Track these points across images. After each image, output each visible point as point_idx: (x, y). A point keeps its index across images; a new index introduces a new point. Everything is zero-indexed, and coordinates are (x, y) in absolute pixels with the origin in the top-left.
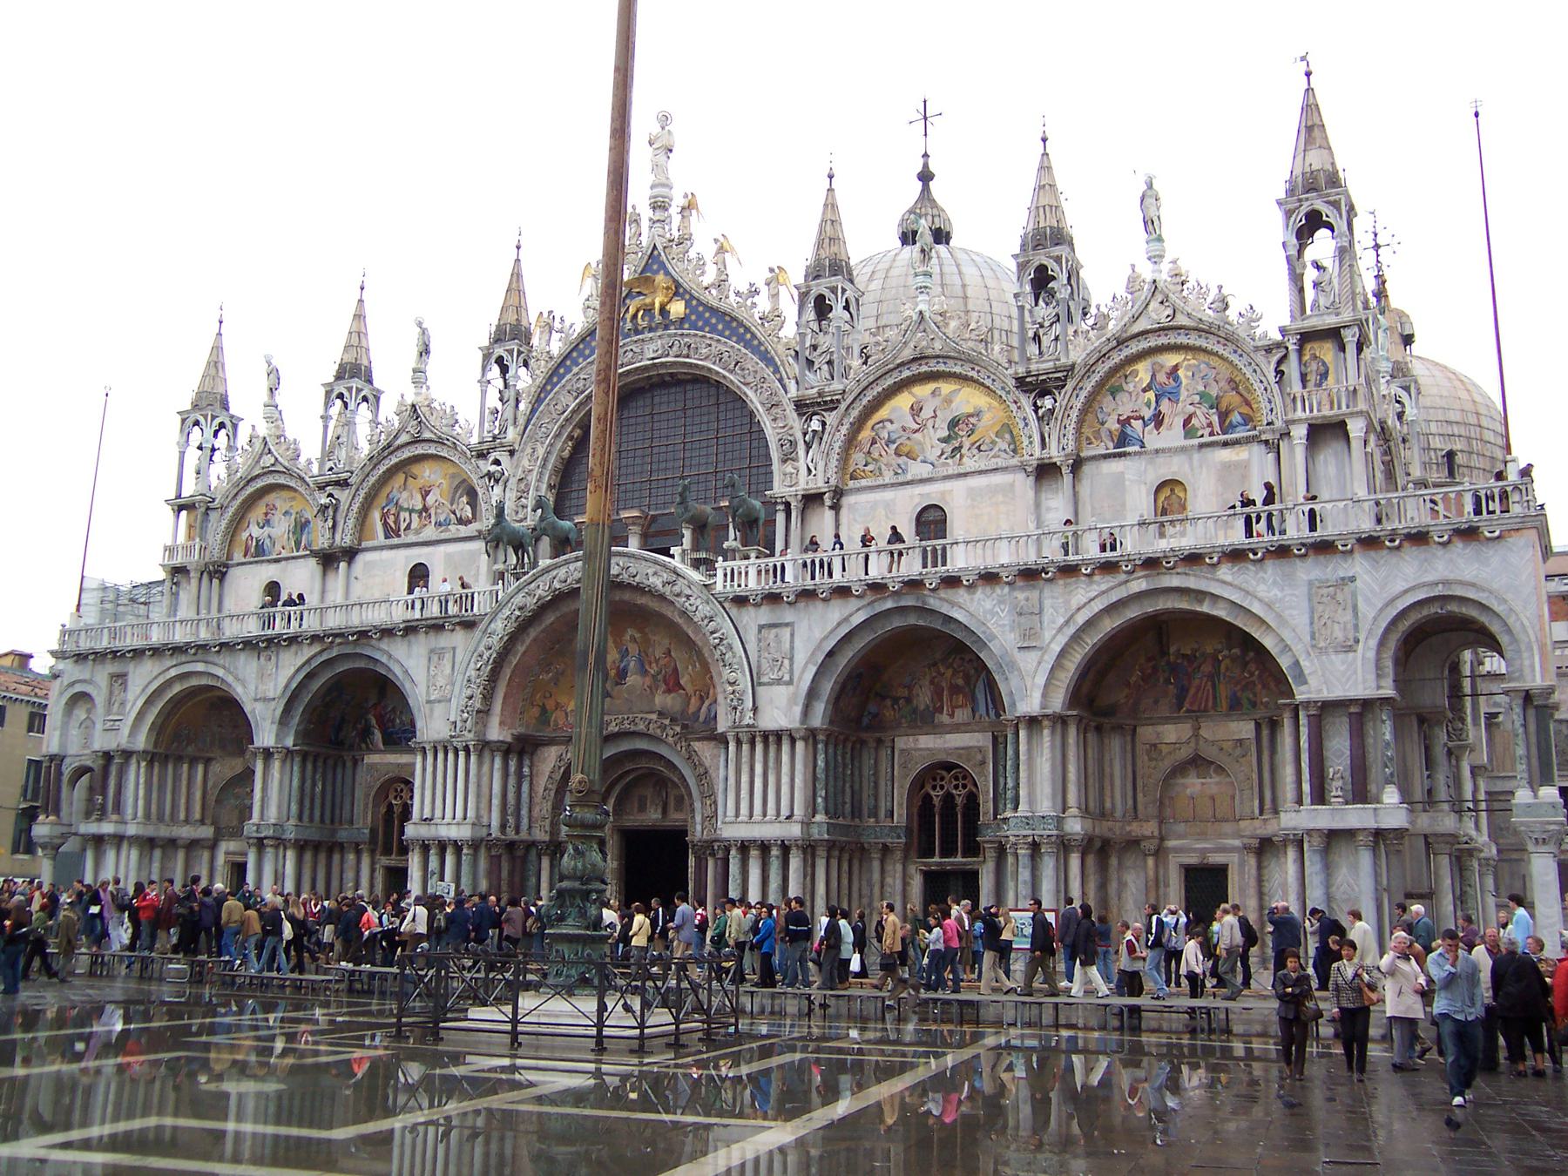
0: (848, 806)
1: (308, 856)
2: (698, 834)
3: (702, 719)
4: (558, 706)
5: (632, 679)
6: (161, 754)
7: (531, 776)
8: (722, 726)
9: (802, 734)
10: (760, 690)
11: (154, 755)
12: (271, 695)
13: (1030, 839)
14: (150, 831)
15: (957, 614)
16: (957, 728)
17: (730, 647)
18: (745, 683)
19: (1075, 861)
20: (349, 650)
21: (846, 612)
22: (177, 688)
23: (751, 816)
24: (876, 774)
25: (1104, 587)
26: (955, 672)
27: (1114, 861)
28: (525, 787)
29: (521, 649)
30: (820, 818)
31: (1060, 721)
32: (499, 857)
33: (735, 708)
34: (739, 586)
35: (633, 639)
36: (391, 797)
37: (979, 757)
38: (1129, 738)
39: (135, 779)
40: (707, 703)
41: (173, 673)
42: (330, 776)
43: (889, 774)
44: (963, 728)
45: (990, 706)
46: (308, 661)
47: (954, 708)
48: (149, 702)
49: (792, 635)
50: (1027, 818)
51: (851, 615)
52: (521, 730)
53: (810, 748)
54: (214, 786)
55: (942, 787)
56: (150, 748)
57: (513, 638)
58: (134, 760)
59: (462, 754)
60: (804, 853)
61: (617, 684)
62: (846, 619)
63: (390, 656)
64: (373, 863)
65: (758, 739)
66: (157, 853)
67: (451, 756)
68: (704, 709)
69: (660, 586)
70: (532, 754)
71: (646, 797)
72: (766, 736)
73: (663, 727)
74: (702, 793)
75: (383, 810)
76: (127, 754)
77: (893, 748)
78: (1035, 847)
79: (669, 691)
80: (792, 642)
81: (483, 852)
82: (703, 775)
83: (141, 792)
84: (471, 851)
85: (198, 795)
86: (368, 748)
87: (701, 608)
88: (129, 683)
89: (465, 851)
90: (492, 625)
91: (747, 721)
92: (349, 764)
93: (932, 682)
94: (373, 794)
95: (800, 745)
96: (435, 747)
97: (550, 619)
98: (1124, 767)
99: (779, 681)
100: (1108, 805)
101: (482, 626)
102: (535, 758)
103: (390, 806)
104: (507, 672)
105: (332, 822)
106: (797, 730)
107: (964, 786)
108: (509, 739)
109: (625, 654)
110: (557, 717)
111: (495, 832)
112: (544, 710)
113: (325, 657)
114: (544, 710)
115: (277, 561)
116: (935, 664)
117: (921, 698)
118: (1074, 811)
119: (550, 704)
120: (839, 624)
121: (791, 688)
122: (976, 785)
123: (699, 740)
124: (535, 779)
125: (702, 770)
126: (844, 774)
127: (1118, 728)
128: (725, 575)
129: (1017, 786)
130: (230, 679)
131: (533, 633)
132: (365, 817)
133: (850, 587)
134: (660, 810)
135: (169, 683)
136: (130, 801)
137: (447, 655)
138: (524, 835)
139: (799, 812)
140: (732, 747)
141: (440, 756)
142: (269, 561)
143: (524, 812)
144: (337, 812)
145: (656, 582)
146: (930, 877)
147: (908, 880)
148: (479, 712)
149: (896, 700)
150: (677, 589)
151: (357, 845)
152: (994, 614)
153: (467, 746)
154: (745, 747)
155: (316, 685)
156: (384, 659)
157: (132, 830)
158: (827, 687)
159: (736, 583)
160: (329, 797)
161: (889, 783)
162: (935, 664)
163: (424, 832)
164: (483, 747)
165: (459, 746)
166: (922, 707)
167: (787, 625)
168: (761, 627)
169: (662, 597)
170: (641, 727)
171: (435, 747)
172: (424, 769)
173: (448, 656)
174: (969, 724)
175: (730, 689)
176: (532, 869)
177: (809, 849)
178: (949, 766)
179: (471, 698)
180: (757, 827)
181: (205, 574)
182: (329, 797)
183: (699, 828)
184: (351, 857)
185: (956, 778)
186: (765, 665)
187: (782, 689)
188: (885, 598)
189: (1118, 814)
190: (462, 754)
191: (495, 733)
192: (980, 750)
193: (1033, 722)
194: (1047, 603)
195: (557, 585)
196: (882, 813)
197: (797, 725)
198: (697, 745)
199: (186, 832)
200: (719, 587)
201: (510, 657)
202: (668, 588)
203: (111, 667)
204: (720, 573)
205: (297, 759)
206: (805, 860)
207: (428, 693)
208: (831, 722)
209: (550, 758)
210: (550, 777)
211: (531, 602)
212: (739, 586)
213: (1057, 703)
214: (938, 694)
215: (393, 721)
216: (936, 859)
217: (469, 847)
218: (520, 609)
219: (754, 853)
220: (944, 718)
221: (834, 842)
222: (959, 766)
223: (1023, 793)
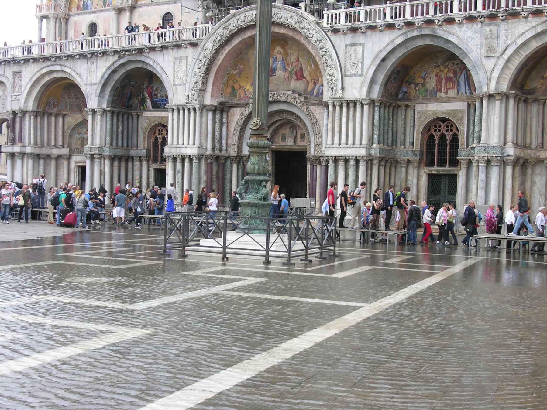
0: (390, 140)
1: (116, 163)
2: (312, 153)
3: (315, 94)
4: (240, 87)
7: (227, 123)
8: (326, 97)
9: (367, 102)
10: (346, 79)
13: (486, 158)
14: (37, 151)
15: (451, 38)
16: (448, 100)
17: (330, 56)
18: (338, 75)
19: (509, 170)
20: (132, 58)
21: (392, 37)
22: (47, 79)
23: (340, 144)
24: (405, 123)
25: (534, 24)
26: (449, 70)
27: (529, 171)
28: (224, 129)
29: (221, 57)
30: (375, 145)
31: (506, 96)
32: (212, 164)
33: (333, 88)
34: (336, 23)
35: (279, 52)
36: (157, 134)
37: (460, 115)
38: (541, 106)
39: (29, 124)
40: (317, 86)
41: (45, 71)
42: (125, 123)
43: (412, 123)
44: (452, 100)
45: (467, 88)
46: (113, 64)
47: (447, 89)
48: (33, 86)
49: (363, 50)
50: (485, 147)
51: (394, 39)
52: (223, 100)
53: (371, 109)
54: (68, 129)
55: (440, 131)
56: (35, 109)
57: (217, 52)
58: (27, 115)
59: (192, 112)
60: (367, 163)
62: (393, 41)
63: (154, 61)
64: (148, 167)
65: (344, 105)
66: (42, 161)
68: (316, 89)
69: (293, 24)
70: (228, 112)
71: (285, 134)
72: (348, 104)
73: (295, 99)
74: (314, 132)
75: (153, 140)
76: (24, 112)
77: (415, 110)
78: (488, 162)
79: (298, 79)
80: (363, 53)
81: (203, 162)
82: (315, 124)
83: (32, 131)
84: (197, 161)
85: (60, 132)
86: (144, 109)
87: (315, 34)
88: (23, 76)
89: (194, 161)
90: (206, 45)
91: (339, 95)
92: (135, 118)
93: (436, 76)
94: (147, 132)
95: (366, 108)
96: (178, 108)
97: (236, 42)
98: (538, 122)
99: (355, 74)
100: (528, 141)
101: (201, 45)
102: (229, 114)
103: (156, 138)
104: (214, 70)
105: (128, 146)
106: (365, 100)
107: (451, 130)
108: (216, 104)
110: (240, 93)
111: (209, 152)
112: (233, 89)
113: (121, 61)
114: (233, 89)
115: (95, 12)
116: (438, 66)
117: (430, 84)
118: (510, 144)
119: (236, 86)
120: (388, 44)
121: (362, 78)
122: (457, 130)
123: (313, 105)
124: (229, 124)
125: (315, 121)
126: (388, 123)
127: (536, 101)
128: (328, 18)
129: (480, 131)
130: (73, 74)
131: (228, 49)
132: (144, 144)
133: (394, 24)
134: (293, 141)
135: (43, 76)
136: (27, 136)
137: (183, 61)
138: (224, 153)
139: (365, 141)
140: (331, 109)
141: (181, 113)
142: (90, 13)
143: (224, 141)
144: (130, 141)
145: (292, 22)
147: (420, 178)
148: (200, 90)
149: (416, 85)
150: (302, 25)
151: (140, 157)
152: (473, 38)
154: (338, 109)
155: (117, 76)
156: (151, 63)
157: (28, 150)
158: (381, 78)
159: (334, 22)
160: (125, 133)
161: (412, 128)
162: (438, 66)
163: (174, 151)
164: (203, 108)
165: (191, 108)
166: (430, 89)
167: (361, 44)
168: (347, 46)
169: (294, 29)
170: (283, 98)
171: (178, 108)
172: (173, 120)
173: (184, 61)
174: (456, 98)
175: (330, 78)
176: (228, 170)
177: (369, 161)
178: (444, 120)
179: (196, 83)
180: (343, 149)
181: (58, 20)
182: (125, 133)
183: (313, 150)
184: (137, 164)
185: (447, 126)
186: (348, 66)
187: (358, 78)
188: (413, 30)
189: (533, 146)
191: (208, 101)
192: (461, 111)
193: (491, 96)
194: (502, 33)
195: (239, 23)
196: (407, 144)
197: (365, 97)
198: (312, 108)
199: (55, 152)
200: (325, 24)
201: (216, 62)
202: (298, 25)
204: (325, 16)
205: (109, 114)
206: (367, 167)
207: (174, 80)
208: (383, 96)
211: (226, 33)
212: (336, 23)
213: (504, 87)
214: (439, 81)
215: (156, 95)
216: (435, 167)
217: (196, 159)
218: (221, 36)
219: (341, 163)
220: (442, 95)
221: (382, 158)
222: (449, 120)
223: (483, 134)
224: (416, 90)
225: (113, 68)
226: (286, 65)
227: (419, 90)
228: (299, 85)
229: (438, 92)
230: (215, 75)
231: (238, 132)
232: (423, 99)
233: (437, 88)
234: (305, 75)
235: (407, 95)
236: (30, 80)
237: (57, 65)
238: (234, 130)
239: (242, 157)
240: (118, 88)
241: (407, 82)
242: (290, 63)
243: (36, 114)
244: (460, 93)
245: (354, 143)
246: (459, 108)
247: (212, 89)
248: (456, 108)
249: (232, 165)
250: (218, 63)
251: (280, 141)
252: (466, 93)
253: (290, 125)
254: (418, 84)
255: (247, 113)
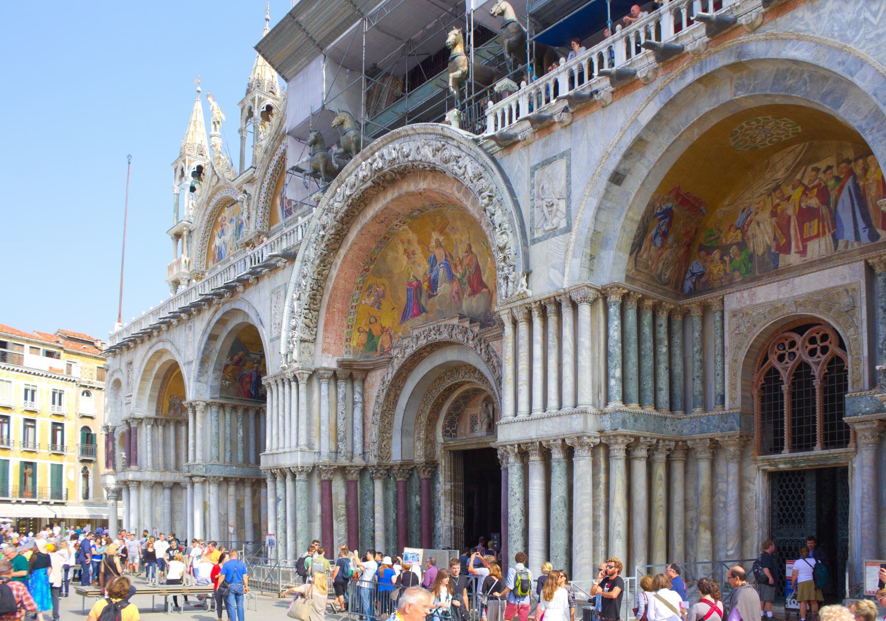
4: (383, 330)
5: (444, 288)
6: (162, 419)
7: (364, 402)
10: (536, 251)
11: (156, 420)
12: (191, 358)
22: (158, 366)
45: (861, 225)
46: (208, 324)
47: (805, 241)
48: (143, 379)
59: (293, 384)
61: (430, 296)
65: (535, 314)
67: (287, 387)
70: (364, 381)
73: (465, 331)
79: (474, 293)
81: (316, 482)
95: (585, 310)
96: (276, 381)
99: (553, 232)
102: (366, 385)
106: (578, 288)
108: (334, 365)
109: (433, 262)
113: (218, 316)
119: (376, 329)
130: (173, 351)
134: (485, 427)
140: (508, 330)
141: (281, 388)
146: (776, 479)
148: (303, 341)
149: (725, 250)
153: (295, 376)
154: (523, 327)
166: (760, 251)
170: (445, 336)
171: (276, 381)
179: (294, 328)
187: (559, 240)
190: (293, 384)
201: (328, 283)
203: (126, 357)
205: (214, 409)
209: (377, 382)
210: (376, 401)
220: (793, 258)
224: (723, 262)
225: (209, 330)
226: (453, 267)
227: (731, 260)
228: (471, 304)
229: (781, 255)
230: (328, 309)
231: (378, 417)
232: (744, 282)
233: (778, 245)
234: (484, 279)
235: (703, 279)
236: (140, 371)
237: (160, 341)
238: (374, 415)
239: (392, 467)
240: (227, 366)
241: (702, 248)
242: (458, 263)
243: (155, 422)
244: (841, 243)
245: (560, 407)
246: (840, 283)
247: (325, 337)
248: (832, 285)
249: (373, 483)
250: (330, 284)
251: (468, 430)
252: (857, 238)
253: (483, 397)
254: (731, 245)
255: (390, 377)
